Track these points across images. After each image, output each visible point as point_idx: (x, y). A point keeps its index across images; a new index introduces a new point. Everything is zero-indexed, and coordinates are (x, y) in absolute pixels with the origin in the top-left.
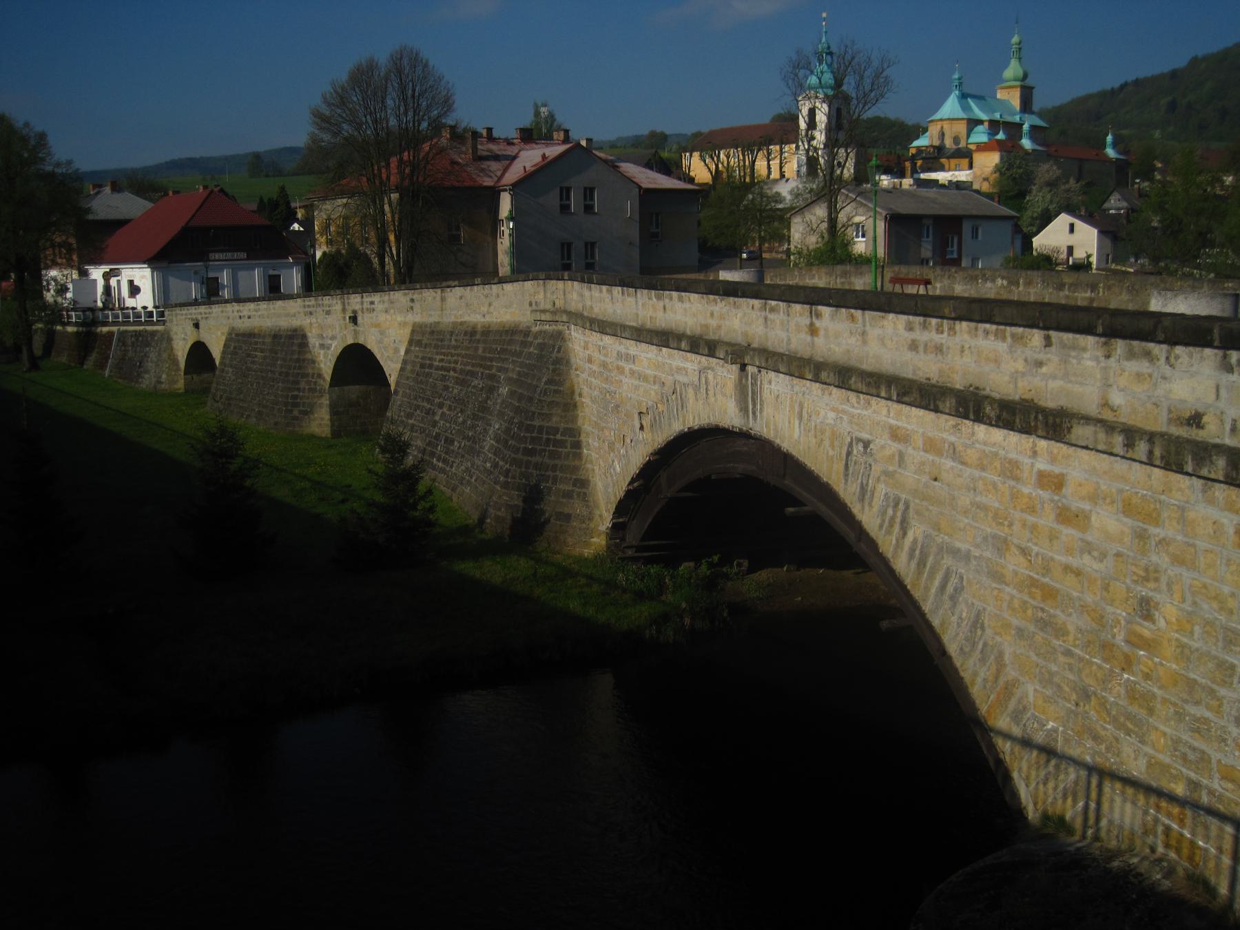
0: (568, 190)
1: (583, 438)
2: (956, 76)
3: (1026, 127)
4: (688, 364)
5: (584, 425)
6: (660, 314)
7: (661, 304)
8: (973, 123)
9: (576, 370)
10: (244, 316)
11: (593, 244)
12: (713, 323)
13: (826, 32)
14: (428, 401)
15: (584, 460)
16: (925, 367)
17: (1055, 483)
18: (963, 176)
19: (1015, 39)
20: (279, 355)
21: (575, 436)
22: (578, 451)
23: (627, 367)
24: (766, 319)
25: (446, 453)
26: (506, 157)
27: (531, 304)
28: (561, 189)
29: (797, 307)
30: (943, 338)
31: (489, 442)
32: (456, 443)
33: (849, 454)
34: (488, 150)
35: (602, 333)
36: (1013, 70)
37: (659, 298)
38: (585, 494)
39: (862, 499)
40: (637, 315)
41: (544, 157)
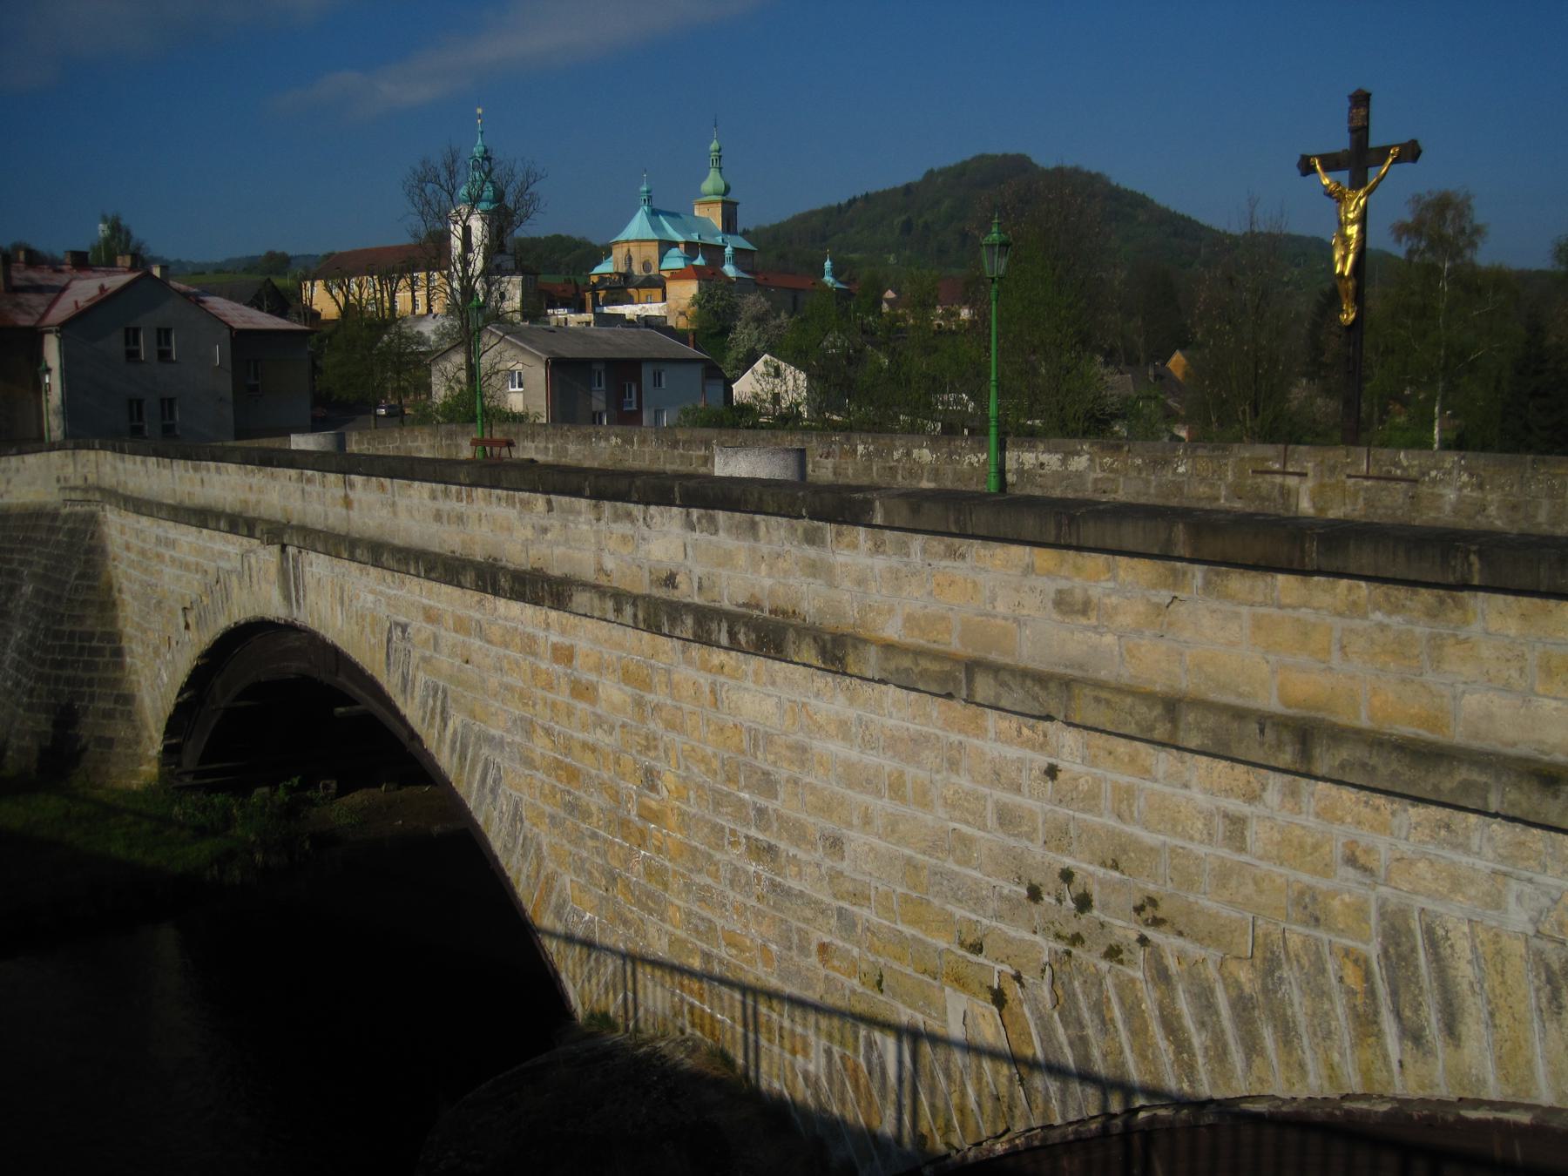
0: (136, 331)
1: (125, 644)
2: (644, 188)
3: (728, 250)
4: (227, 547)
5: (125, 626)
6: (198, 489)
7: (198, 476)
8: (666, 245)
9: (114, 560)
11: (171, 401)
12: (252, 498)
13: (482, 132)
15: (127, 671)
17: (564, 655)
18: (654, 309)
19: (714, 146)
21: (114, 642)
22: (119, 660)
23: (168, 553)
24: (303, 491)
26: (52, 289)
27: (58, 480)
28: (127, 330)
30: (461, 507)
33: (389, 640)
34: (27, 279)
35: (138, 513)
36: (712, 182)
37: (196, 469)
38: (130, 712)
39: (404, 691)
40: (174, 490)
41: (102, 288)
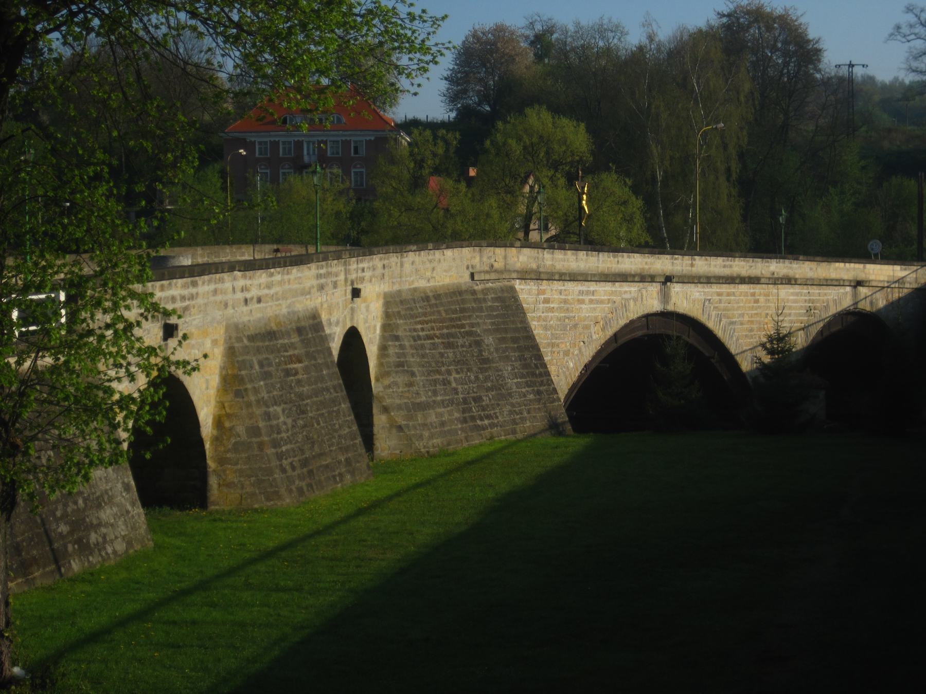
4: (631, 289)
7: (616, 259)
10: (252, 299)
12: (647, 267)
14: (439, 372)
16: (727, 272)
20: (320, 361)
23: (587, 298)
25: (484, 410)
27: (468, 268)
29: (687, 257)
31: (511, 382)
32: (484, 398)
37: (614, 257)
40: (598, 267)
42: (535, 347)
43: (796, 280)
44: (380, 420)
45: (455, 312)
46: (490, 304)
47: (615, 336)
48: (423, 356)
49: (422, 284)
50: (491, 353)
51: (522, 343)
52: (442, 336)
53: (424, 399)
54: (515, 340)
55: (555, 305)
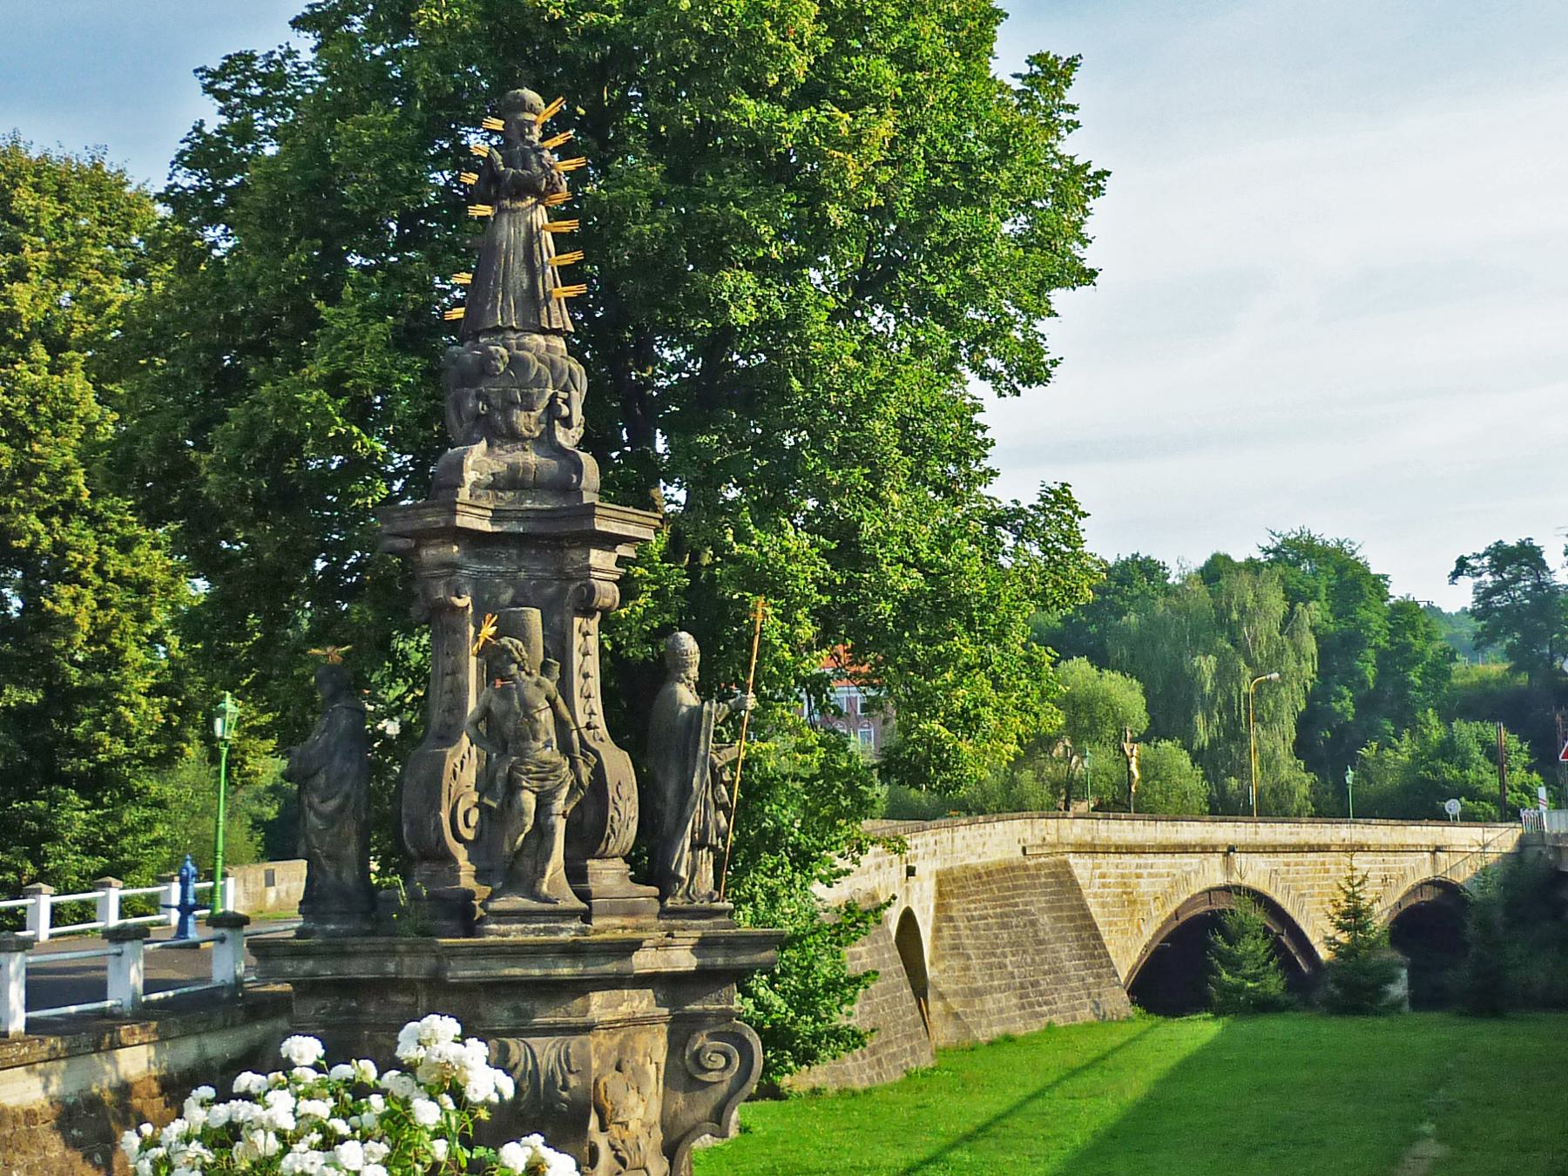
4: (1192, 861)
12: (1208, 836)
14: (994, 955)
16: (1293, 840)
23: (1145, 872)
25: (1041, 995)
42: (1094, 927)
43: (1369, 846)
44: (935, 1006)
45: (1008, 889)
46: (1043, 880)
47: (1176, 914)
48: (977, 938)
49: (973, 861)
50: (1046, 934)
51: (1079, 923)
52: (996, 916)
53: (980, 983)
54: (1071, 919)
55: (1112, 881)
